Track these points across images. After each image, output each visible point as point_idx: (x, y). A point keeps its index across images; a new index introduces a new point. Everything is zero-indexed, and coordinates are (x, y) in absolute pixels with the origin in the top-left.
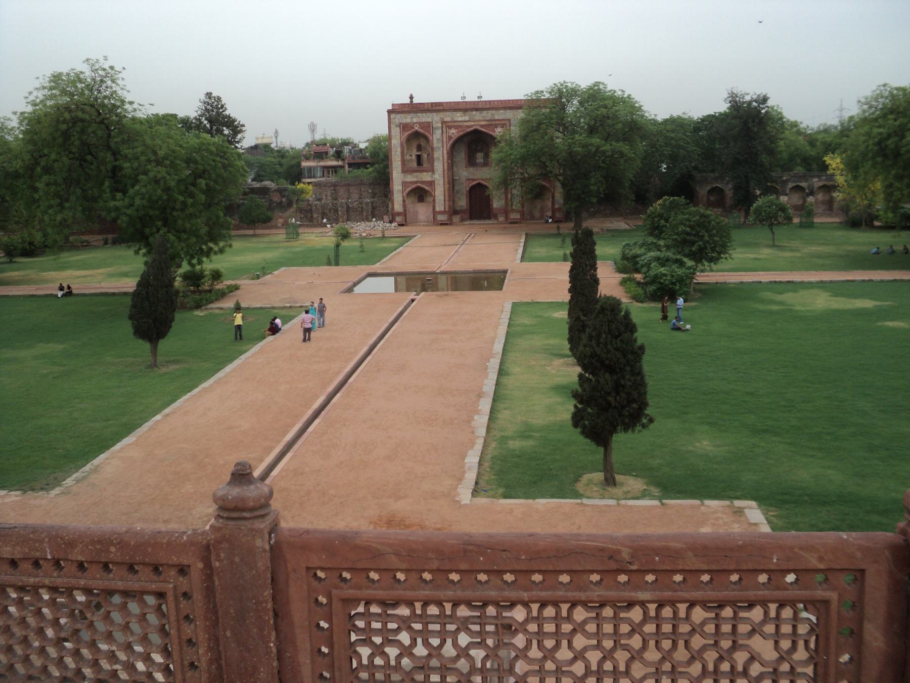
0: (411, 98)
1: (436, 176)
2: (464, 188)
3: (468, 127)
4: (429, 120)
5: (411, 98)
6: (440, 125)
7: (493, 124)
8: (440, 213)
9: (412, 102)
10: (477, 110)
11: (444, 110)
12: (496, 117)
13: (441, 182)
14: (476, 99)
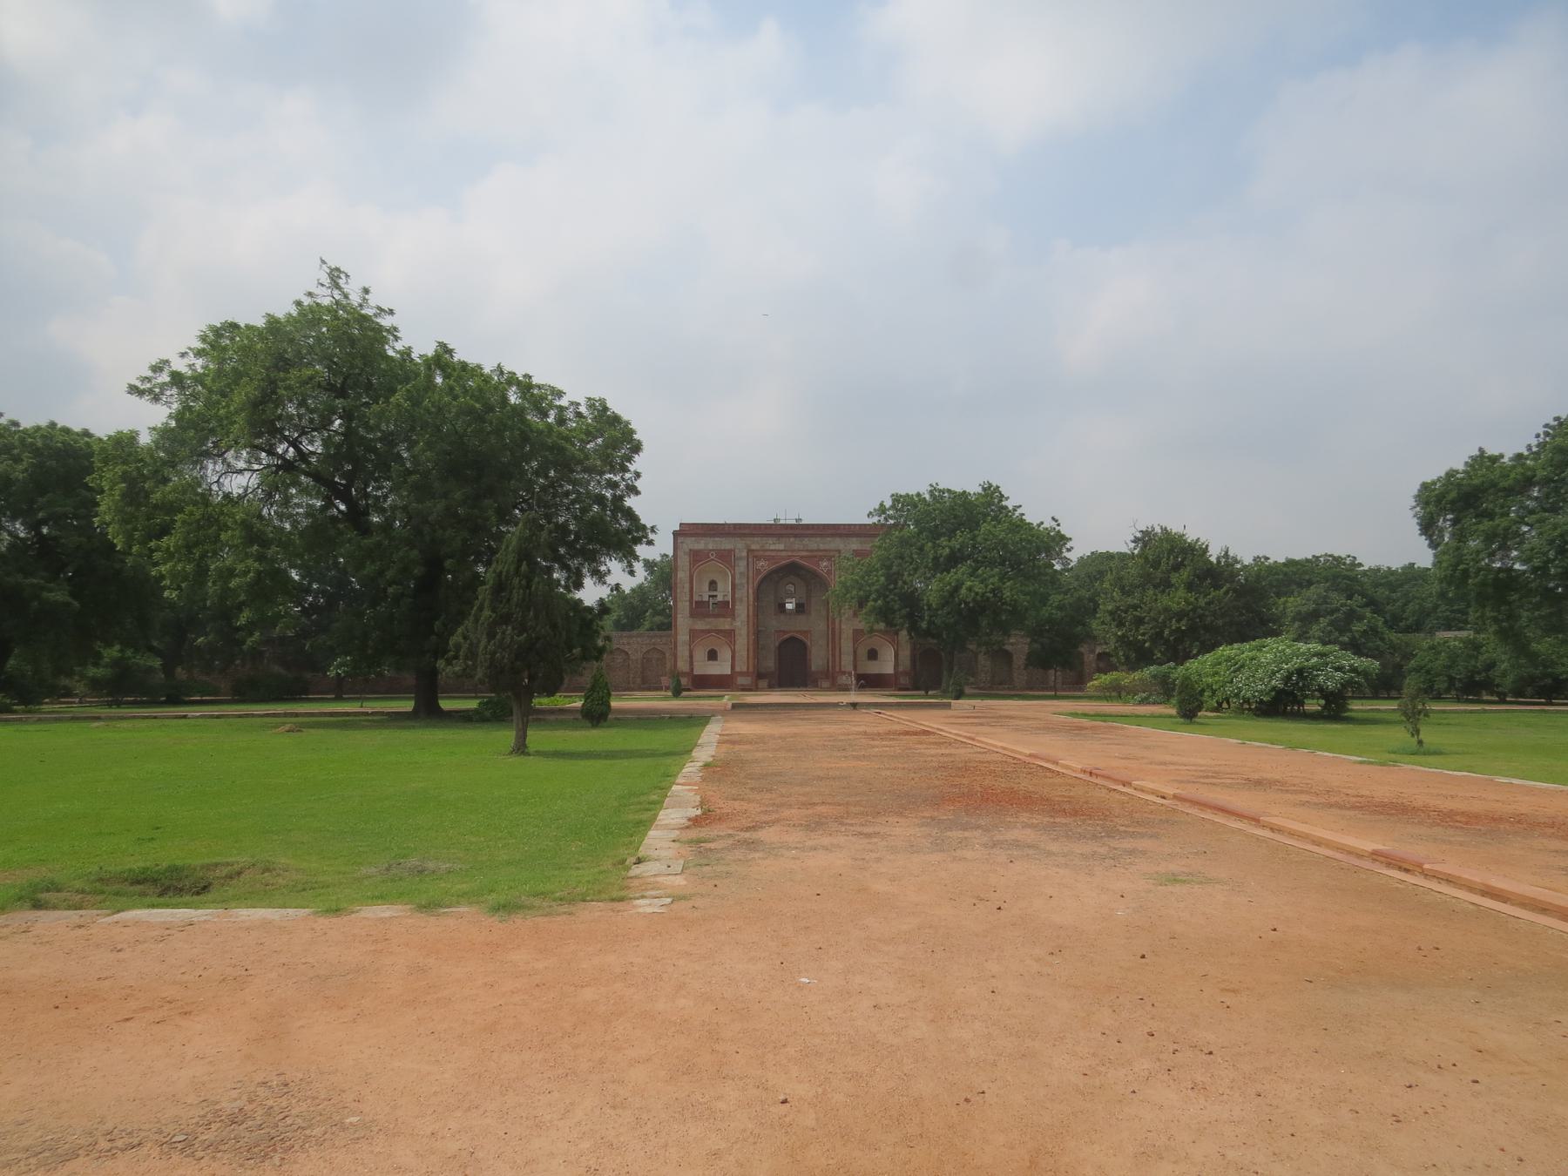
1: (738, 624)
4: (728, 546)
6: (744, 554)
8: (741, 674)
10: (796, 536)
11: (753, 535)
12: (822, 547)
13: (744, 632)
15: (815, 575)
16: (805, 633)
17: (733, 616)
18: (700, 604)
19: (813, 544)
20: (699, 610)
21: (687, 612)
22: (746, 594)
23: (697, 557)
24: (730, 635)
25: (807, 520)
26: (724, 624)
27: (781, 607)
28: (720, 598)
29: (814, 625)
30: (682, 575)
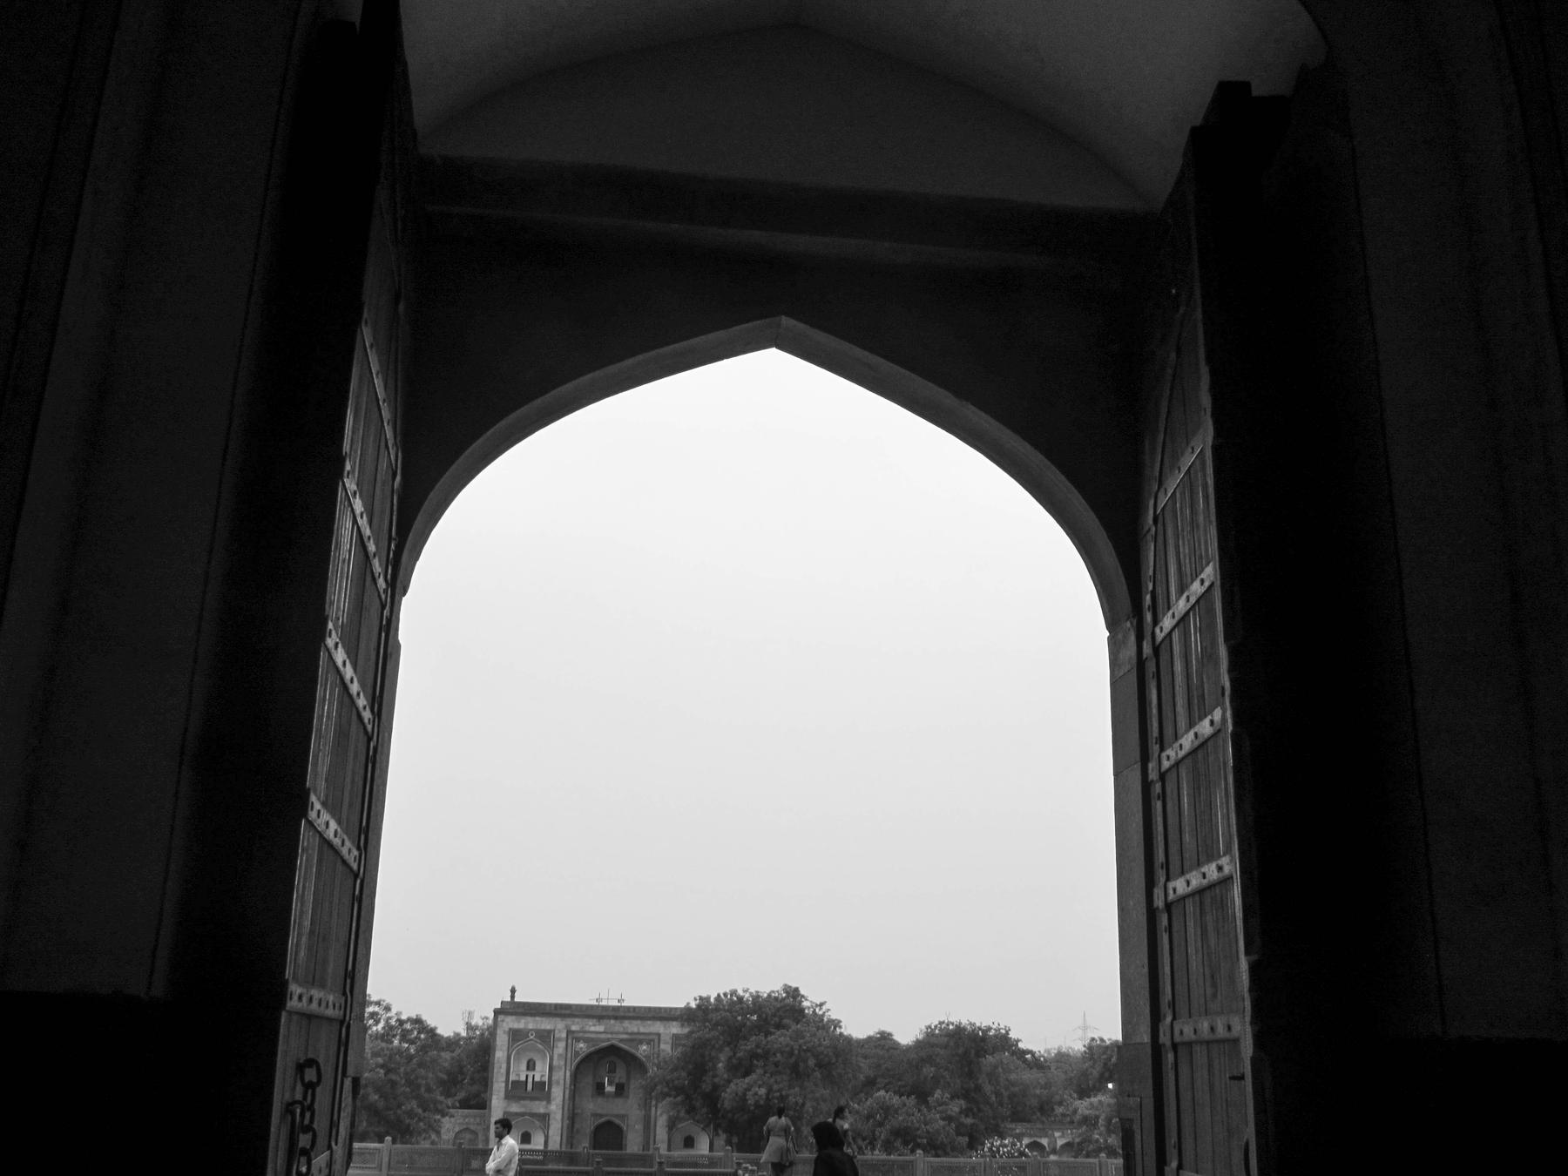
0: (513, 991)
1: (553, 1107)
2: (588, 1126)
3: (603, 1041)
5: (513, 991)
7: (637, 1040)
9: (513, 997)
10: (616, 1018)
13: (559, 1117)
14: (615, 1003)
15: (634, 1058)
16: (622, 1117)
17: (548, 1098)
18: (516, 1083)
19: (634, 1027)
20: (516, 1091)
21: (502, 1094)
22: (563, 1076)
23: (515, 1035)
24: (544, 1118)
25: (629, 1002)
26: (539, 1107)
27: (600, 1088)
28: (537, 1079)
29: (629, 1110)
30: (500, 1055)
